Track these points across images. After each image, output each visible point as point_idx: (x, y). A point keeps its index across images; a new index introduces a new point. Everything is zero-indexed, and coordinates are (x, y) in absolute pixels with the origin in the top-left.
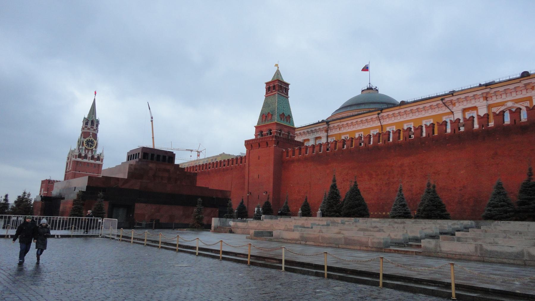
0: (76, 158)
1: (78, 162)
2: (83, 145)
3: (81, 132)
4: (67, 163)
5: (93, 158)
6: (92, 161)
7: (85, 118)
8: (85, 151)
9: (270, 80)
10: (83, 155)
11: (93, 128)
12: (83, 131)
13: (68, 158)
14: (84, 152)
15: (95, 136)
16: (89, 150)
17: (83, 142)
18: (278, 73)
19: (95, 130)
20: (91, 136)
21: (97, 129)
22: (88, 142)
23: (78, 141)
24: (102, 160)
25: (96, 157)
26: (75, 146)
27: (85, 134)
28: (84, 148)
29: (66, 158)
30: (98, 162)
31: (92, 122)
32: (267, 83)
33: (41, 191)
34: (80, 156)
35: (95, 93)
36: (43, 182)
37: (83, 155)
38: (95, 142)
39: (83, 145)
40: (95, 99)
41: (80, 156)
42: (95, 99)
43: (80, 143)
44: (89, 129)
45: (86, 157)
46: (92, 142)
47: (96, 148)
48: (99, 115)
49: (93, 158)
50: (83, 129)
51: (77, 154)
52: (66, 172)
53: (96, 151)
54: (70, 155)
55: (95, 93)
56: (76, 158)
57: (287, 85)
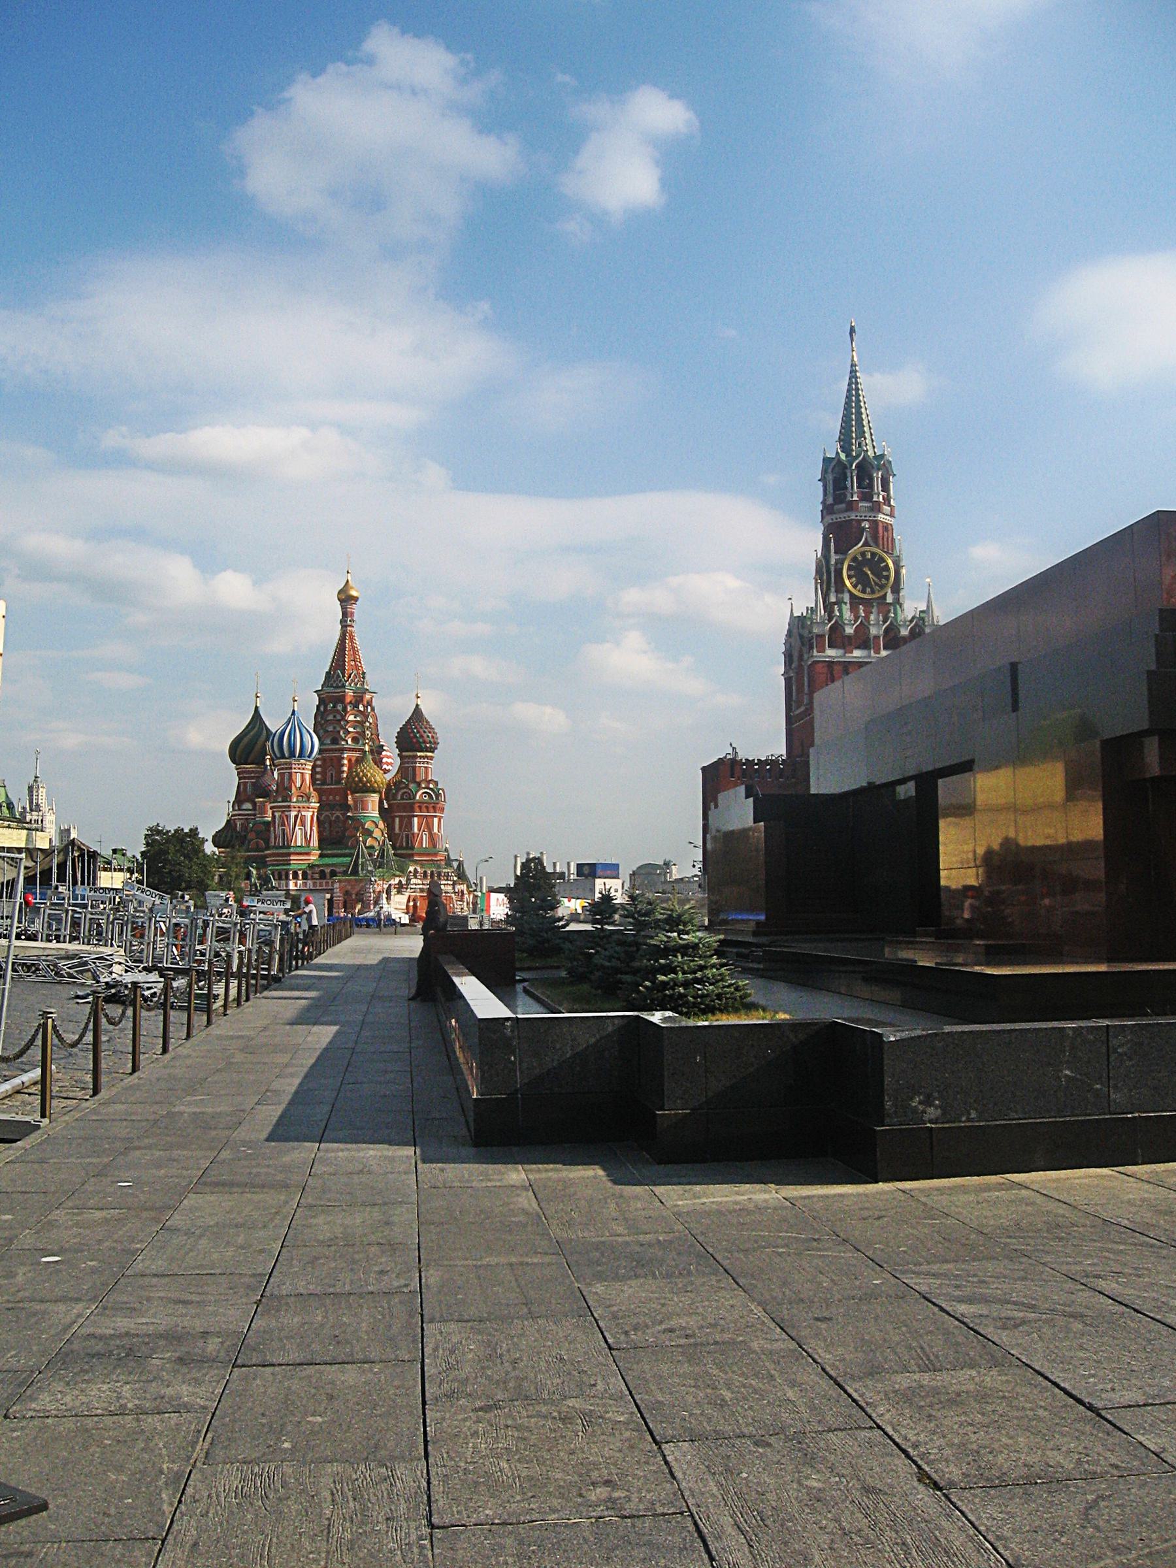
4: (788, 681)
5: (892, 640)
7: (826, 461)
8: (854, 609)
10: (849, 630)
11: (867, 497)
12: (828, 519)
14: (847, 614)
15: (881, 535)
16: (868, 603)
19: (877, 508)
21: (887, 500)
23: (819, 571)
25: (904, 632)
26: (804, 597)
28: (846, 598)
34: (837, 637)
35: (852, 330)
43: (828, 578)
44: (851, 506)
45: (863, 640)
47: (896, 589)
50: (827, 510)
52: (789, 720)
54: (797, 643)
55: (852, 330)
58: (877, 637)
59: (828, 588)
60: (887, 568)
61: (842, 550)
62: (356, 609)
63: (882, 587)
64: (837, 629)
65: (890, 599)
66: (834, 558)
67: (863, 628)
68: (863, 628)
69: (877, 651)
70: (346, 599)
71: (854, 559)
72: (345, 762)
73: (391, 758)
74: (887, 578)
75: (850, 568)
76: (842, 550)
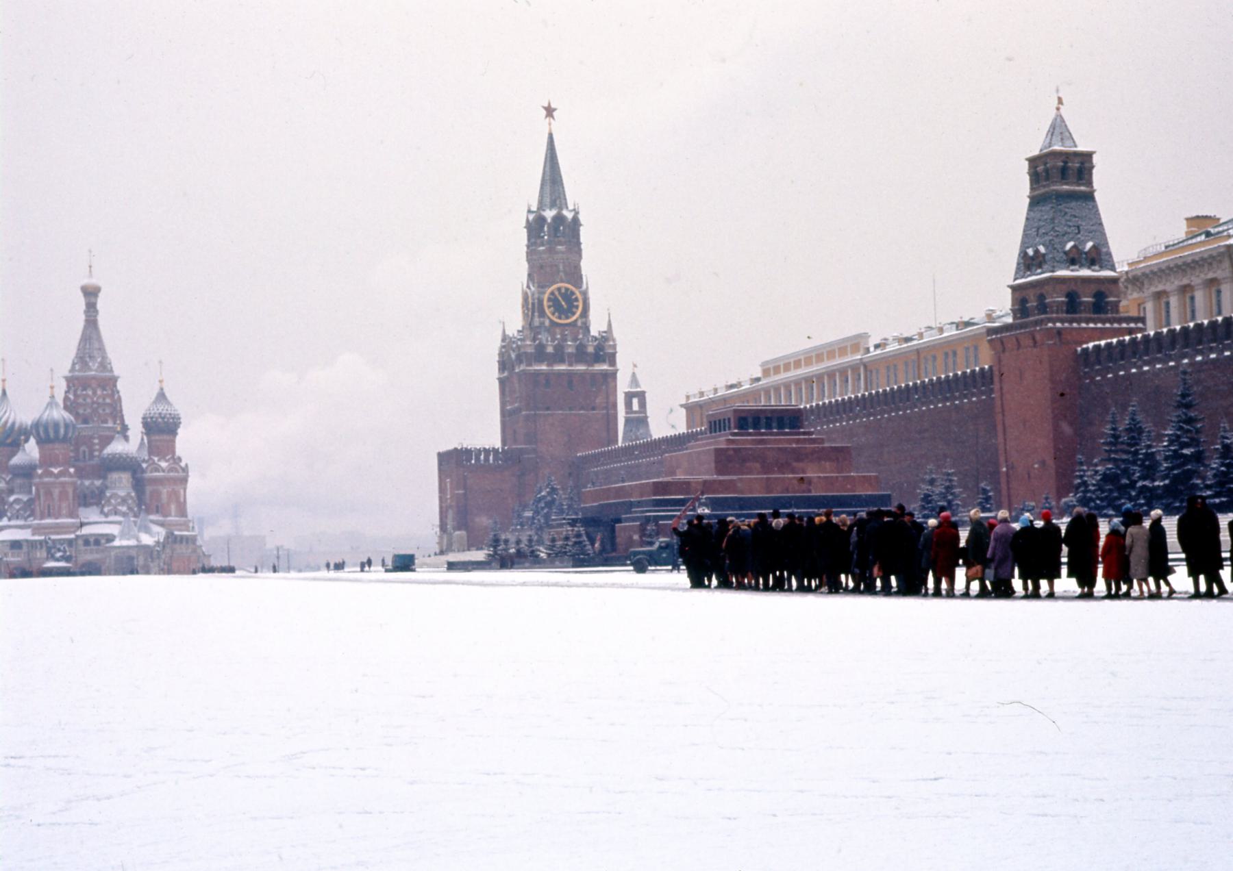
1: (538, 374)
3: (525, 266)
6: (581, 367)
9: (1036, 152)
10: (550, 350)
13: (503, 365)
15: (575, 276)
17: (541, 302)
18: (1058, 128)
22: (554, 300)
24: (612, 361)
25: (590, 349)
27: (540, 271)
28: (547, 323)
29: (496, 366)
31: (559, 219)
32: (1033, 162)
33: (442, 490)
34: (540, 354)
36: (444, 458)
37: (550, 350)
38: (578, 294)
41: (540, 354)
43: (532, 308)
45: (559, 356)
46: (569, 297)
49: (581, 355)
53: (587, 329)
57: (1089, 156)
58: (570, 355)
59: (533, 312)
60: (576, 300)
61: (542, 286)
63: (574, 314)
64: (541, 348)
65: (579, 323)
67: (559, 349)
70: (91, 294)
71: (552, 293)
72: (96, 441)
74: (577, 307)
75: (549, 300)
76: (542, 286)
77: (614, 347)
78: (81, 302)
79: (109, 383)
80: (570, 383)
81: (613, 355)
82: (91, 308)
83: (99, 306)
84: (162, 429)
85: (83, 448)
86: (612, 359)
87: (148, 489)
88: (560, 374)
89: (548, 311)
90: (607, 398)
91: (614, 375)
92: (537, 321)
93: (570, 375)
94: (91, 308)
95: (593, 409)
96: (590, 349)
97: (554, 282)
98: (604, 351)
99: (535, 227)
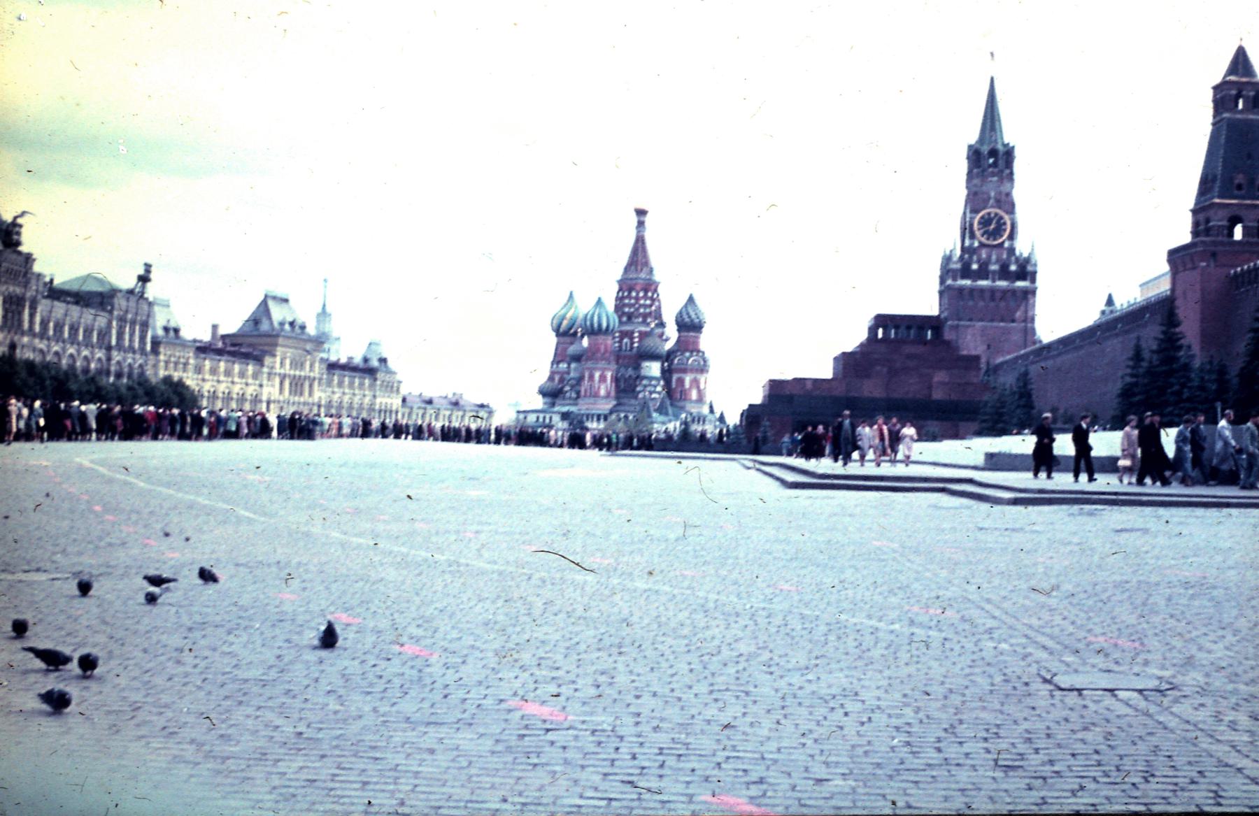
0: (955, 279)
1: (961, 290)
2: (972, 236)
6: (1002, 284)
7: (970, 147)
13: (942, 281)
17: (971, 225)
20: (992, 201)
22: (985, 222)
24: (1033, 281)
27: (975, 200)
28: (976, 244)
30: (1020, 284)
31: (993, 153)
34: (966, 272)
35: (992, 54)
39: (972, 236)
40: (992, 79)
42: (992, 79)
43: (967, 230)
45: (983, 273)
47: (1012, 237)
48: (1010, 134)
49: (1004, 273)
51: (958, 266)
53: (1011, 250)
55: (992, 54)
56: (955, 279)
58: (994, 272)
62: (648, 220)
65: (1007, 245)
66: (968, 215)
67: (984, 266)
68: (984, 266)
69: (994, 281)
70: (641, 213)
71: (982, 217)
73: (672, 332)
75: (980, 223)
77: (1035, 265)
78: (634, 219)
79: (650, 287)
80: (993, 298)
81: (1035, 273)
82: (641, 224)
83: (647, 224)
84: (690, 326)
85: (626, 340)
86: (1032, 277)
87: (675, 377)
88: (982, 290)
89: (978, 233)
90: (1026, 312)
91: (1033, 292)
92: (967, 243)
93: (993, 291)
94: (641, 224)
95: (1013, 321)
96: (1013, 268)
97: (984, 208)
98: (1026, 271)
99: (977, 157)
